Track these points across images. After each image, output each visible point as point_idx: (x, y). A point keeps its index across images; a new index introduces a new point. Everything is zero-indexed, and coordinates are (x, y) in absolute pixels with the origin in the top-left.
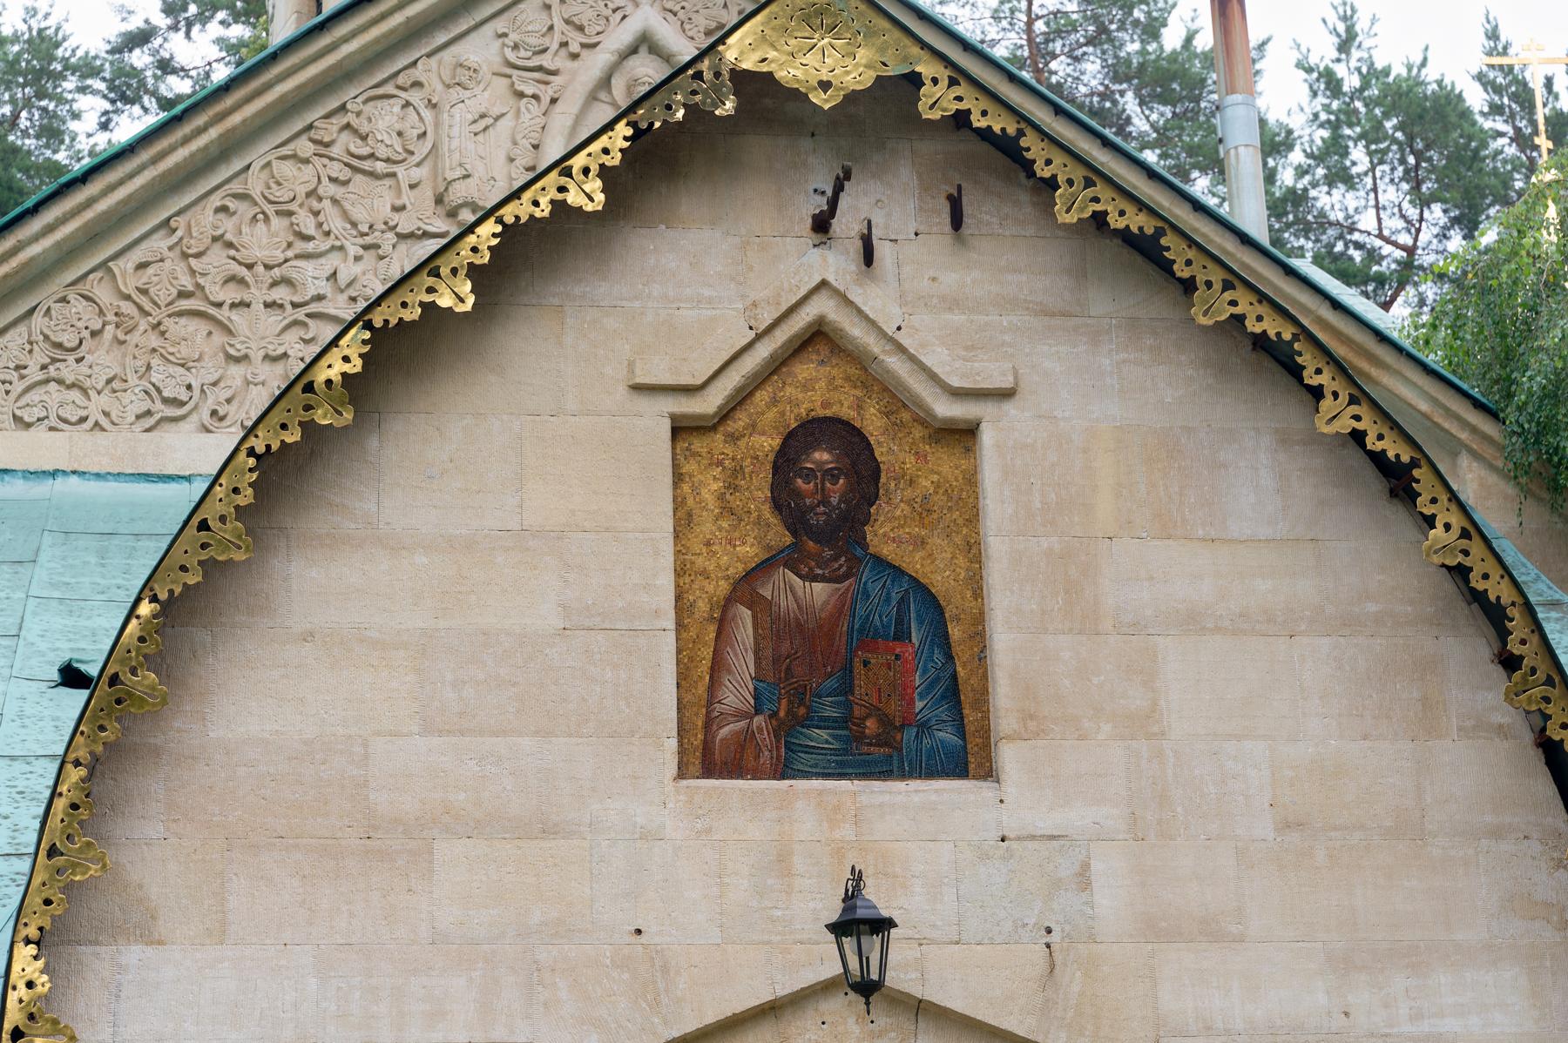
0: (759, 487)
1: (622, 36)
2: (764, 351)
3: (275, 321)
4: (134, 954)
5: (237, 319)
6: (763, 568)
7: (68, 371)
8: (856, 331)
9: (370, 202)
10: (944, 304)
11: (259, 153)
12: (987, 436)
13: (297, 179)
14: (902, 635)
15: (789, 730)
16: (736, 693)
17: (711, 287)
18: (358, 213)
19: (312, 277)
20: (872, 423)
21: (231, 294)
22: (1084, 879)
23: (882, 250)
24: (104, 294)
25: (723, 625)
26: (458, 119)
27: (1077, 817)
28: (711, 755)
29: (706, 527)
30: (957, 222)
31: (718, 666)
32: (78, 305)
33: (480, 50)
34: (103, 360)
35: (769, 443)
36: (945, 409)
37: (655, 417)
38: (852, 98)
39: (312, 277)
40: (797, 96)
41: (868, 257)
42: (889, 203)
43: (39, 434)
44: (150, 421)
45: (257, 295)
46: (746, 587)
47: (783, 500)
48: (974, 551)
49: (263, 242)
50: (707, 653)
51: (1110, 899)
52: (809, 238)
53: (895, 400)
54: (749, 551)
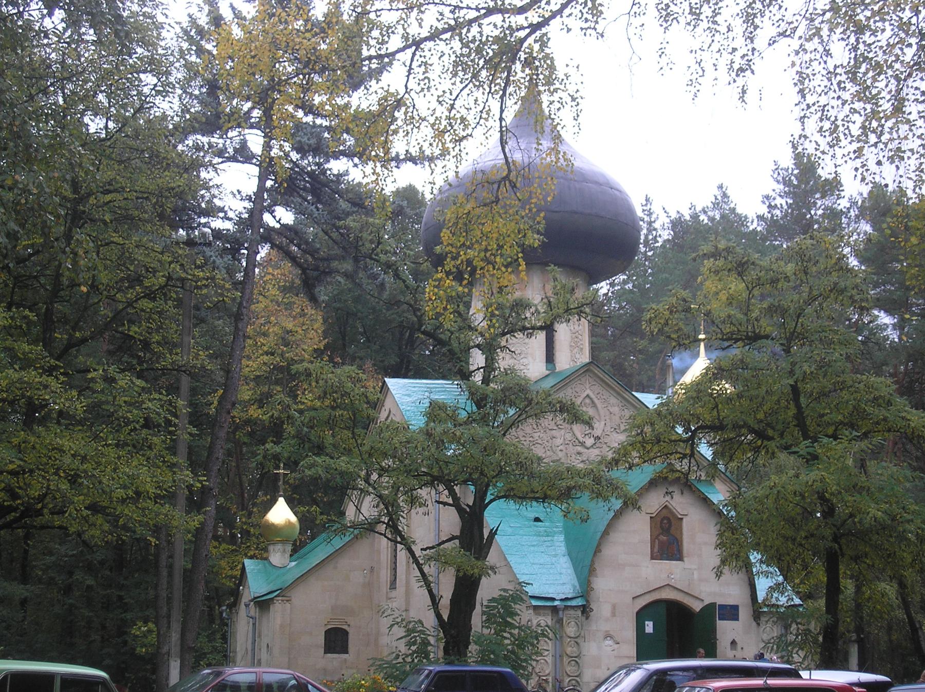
0: (659, 525)
6: (659, 535)
10: (681, 503)
15: (661, 555)
16: (656, 550)
17: (654, 502)
19: (536, 435)
21: (523, 439)
27: (694, 567)
28: (652, 558)
35: (659, 519)
37: (648, 517)
39: (536, 435)
42: (675, 489)
48: (681, 534)
51: (696, 576)
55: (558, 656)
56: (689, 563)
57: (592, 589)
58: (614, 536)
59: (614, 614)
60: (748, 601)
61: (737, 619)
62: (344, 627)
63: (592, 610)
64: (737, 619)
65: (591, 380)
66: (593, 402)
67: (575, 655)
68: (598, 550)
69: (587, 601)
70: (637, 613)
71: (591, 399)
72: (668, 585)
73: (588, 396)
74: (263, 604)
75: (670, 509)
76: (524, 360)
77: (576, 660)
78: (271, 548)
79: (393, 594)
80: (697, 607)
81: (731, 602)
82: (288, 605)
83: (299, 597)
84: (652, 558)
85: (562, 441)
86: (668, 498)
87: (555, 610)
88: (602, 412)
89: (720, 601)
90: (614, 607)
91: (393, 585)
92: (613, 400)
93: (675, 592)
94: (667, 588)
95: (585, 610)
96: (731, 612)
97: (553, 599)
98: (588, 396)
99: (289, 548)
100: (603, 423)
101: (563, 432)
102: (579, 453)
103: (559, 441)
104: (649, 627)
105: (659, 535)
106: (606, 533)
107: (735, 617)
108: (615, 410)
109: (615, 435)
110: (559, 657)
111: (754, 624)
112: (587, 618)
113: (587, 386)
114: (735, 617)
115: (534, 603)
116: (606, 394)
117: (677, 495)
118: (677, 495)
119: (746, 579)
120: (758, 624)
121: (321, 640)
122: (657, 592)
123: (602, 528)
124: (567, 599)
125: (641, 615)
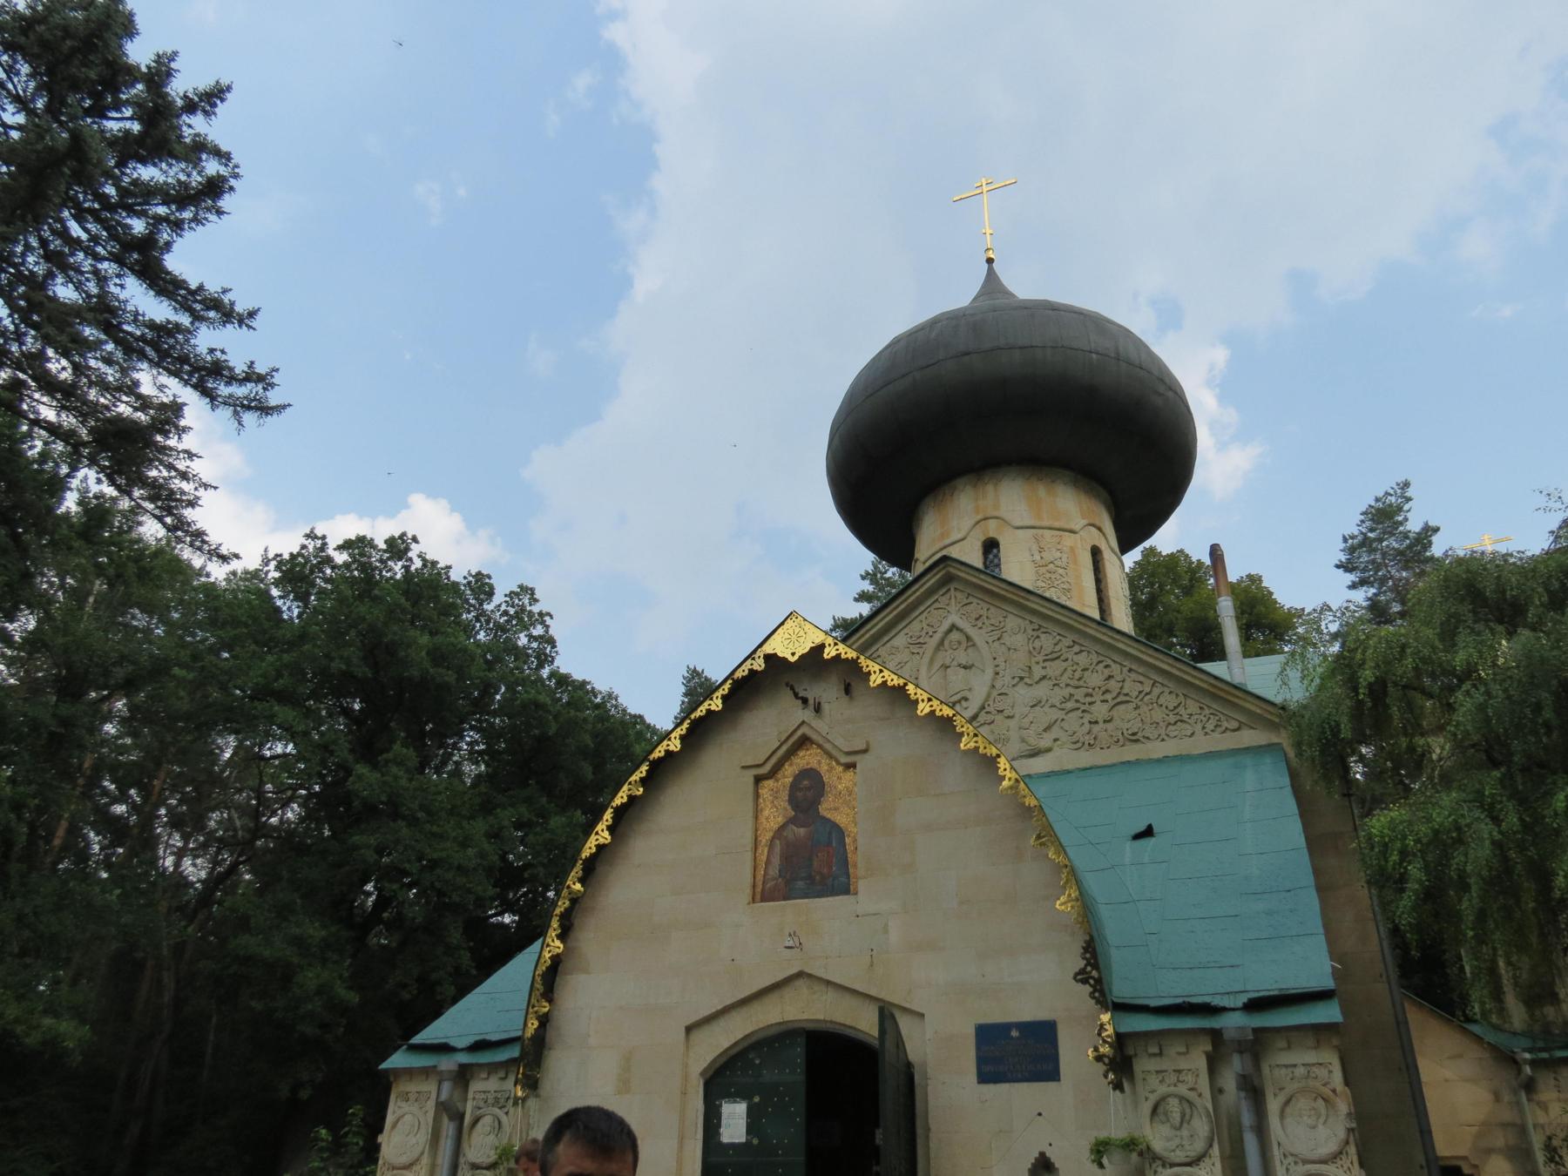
0: (785, 795)
1: (946, 625)
2: (784, 748)
4: (582, 977)
6: (783, 827)
8: (814, 737)
14: (829, 844)
16: (774, 871)
20: (823, 769)
22: (886, 930)
23: (826, 707)
28: (764, 894)
29: (766, 813)
30: (848, 690)
31: (768, 862)
33: (900, 641)
36: (844, 759)
37: (749, 777)
38: (802, 656)
40: (785, 659)
41: (818, 709)
47: (792, 800)
50: (764, 858)
54: (781, 820)
56: (869, 897)
61: (1053, 1075)
64: (1053, 1075)
65: (959, 595)
66: (968, 638)
72: (800, 975)
73: (953, 627)
75: (820, 746)
81: (1027, 1016)
86: (807, 715)
92: (1012, 622)
93: (831, 995)
94: (799, 983)
98: (953, 627)
100: (990, 672)
108: (1019, 640)
109: (1022, 690)
113: (953, 608)
116: (995, 615)
122: (773, 998)
124: (480, 1046)
125: (721, 1081)
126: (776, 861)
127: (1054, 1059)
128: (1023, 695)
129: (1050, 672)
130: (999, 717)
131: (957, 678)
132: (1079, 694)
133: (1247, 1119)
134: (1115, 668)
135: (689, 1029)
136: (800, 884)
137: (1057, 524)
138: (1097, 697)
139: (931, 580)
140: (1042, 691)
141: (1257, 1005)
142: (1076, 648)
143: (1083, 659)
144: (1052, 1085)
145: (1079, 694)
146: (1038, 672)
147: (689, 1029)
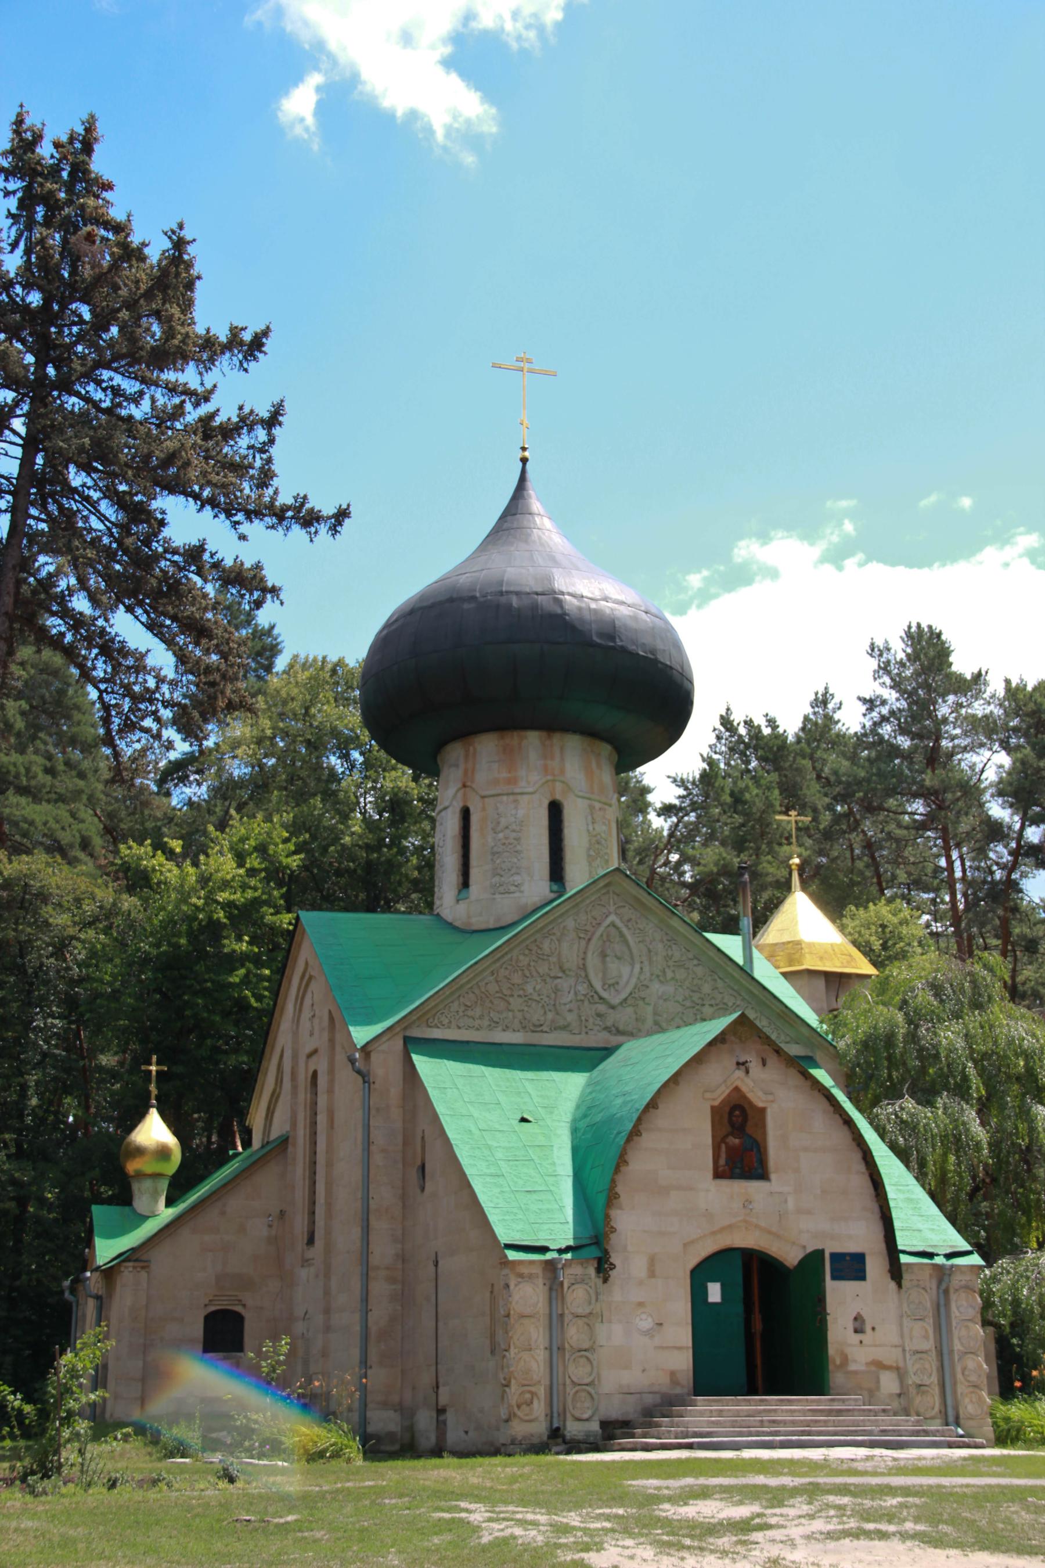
3: (521, 1000)
4: (619, 1212)
5: (511, 1000)
6: (726, 1136)
7: (470, 1013)
9: (543, 969)
11: (515, 953)
12: (769, 1112)
13: (524, 961)
16: (722, 1162)
18: (540, 970)
20: (746, 1106)
22: (786, 1201)
24: (477, 991)
25: (719, 1148)
26: (565, 945)
28: (718, 1175)
30: (764, 1064)
32: (471, 995)
33: (570, 923)
34: (478, 1011)
35: (727, 1109)
36: (761, 1105)
39: (529, 989)
41: (747, 1072)
43: (463, 1031)
44: (490, 1028)
45: (516, 994)
46: (723, 1140)
48: (764, 1133)
49: (517, 979)
51: (791, 1204)
52: (734, 1066)
53: (750, 1103)
55: (555, 1348)
56: (777, 1182)
57: (613, 1230)
58: (647, 1140)
59: (652, 1274)
60: (881, 1246)
61: (863, 1278)
62: (238, 1309)
63: (613, 1267)
64: (863, 1278)
66: (622, 935)
67: (585, 1346)
68: (622, 1160)
69: (606, 1252)
70: (693, 1272)
71: (617, 928)
73: (613, 924)
74: (109, 1273)
76: (516, 878)
77: (586, 1352)
78: (135, 1186)
79: (311, 1253)
80: (791, 1257)
82: (144, 1274)
83: (161, 1259)
84: (718, 1175)
85: (571, 995)
86: (740, 1073)
87: (550, 1265)
88: (635, 951)
89: (830, 1248)
90: (652, 1261)
91: (311, 1241)
95: (603, 1266)
96: (851, 1266)
97: (544, 1249)
99: (164, 1185)
100: (637, 967)
101: (572, 981)
102: (599, 1015)
103: (567, 998)
104: (714, 1293)
105: (726, 1136)
106: (635, 1132)
107: (860, 1275)
110: (556, 1349)
111: (893, 1285)
112: (605, 1280)
113: (612, 909)
114: (860, 1275)
115: (512, 1255)
117: (754, 1066)
118: (754, 1066)
119: (877, 1209)
120: (900, 1285)
121: (198, 1330)
123: (629, 1126)
125: (701, 1274)
126: (723, 1155)
127: (864, 1271)
128: (656, 988)
129: (678, 977)
130: (641, 1003)
131: (613, 966)
132: (696, 997)
133: (942, 1302)
134: (720, 984)
135: (685, 1245)
136: (737, 1171)
137: (603, 800)
138: (707, 1002)
139: (602, 884)
140: (670, 989)
141: (949, 1256)
142: (695, 962)
143: (699, 971)
144: (862, 1283)
145: (696, 997)
146: (669, 974)
147: (685, 1245)
